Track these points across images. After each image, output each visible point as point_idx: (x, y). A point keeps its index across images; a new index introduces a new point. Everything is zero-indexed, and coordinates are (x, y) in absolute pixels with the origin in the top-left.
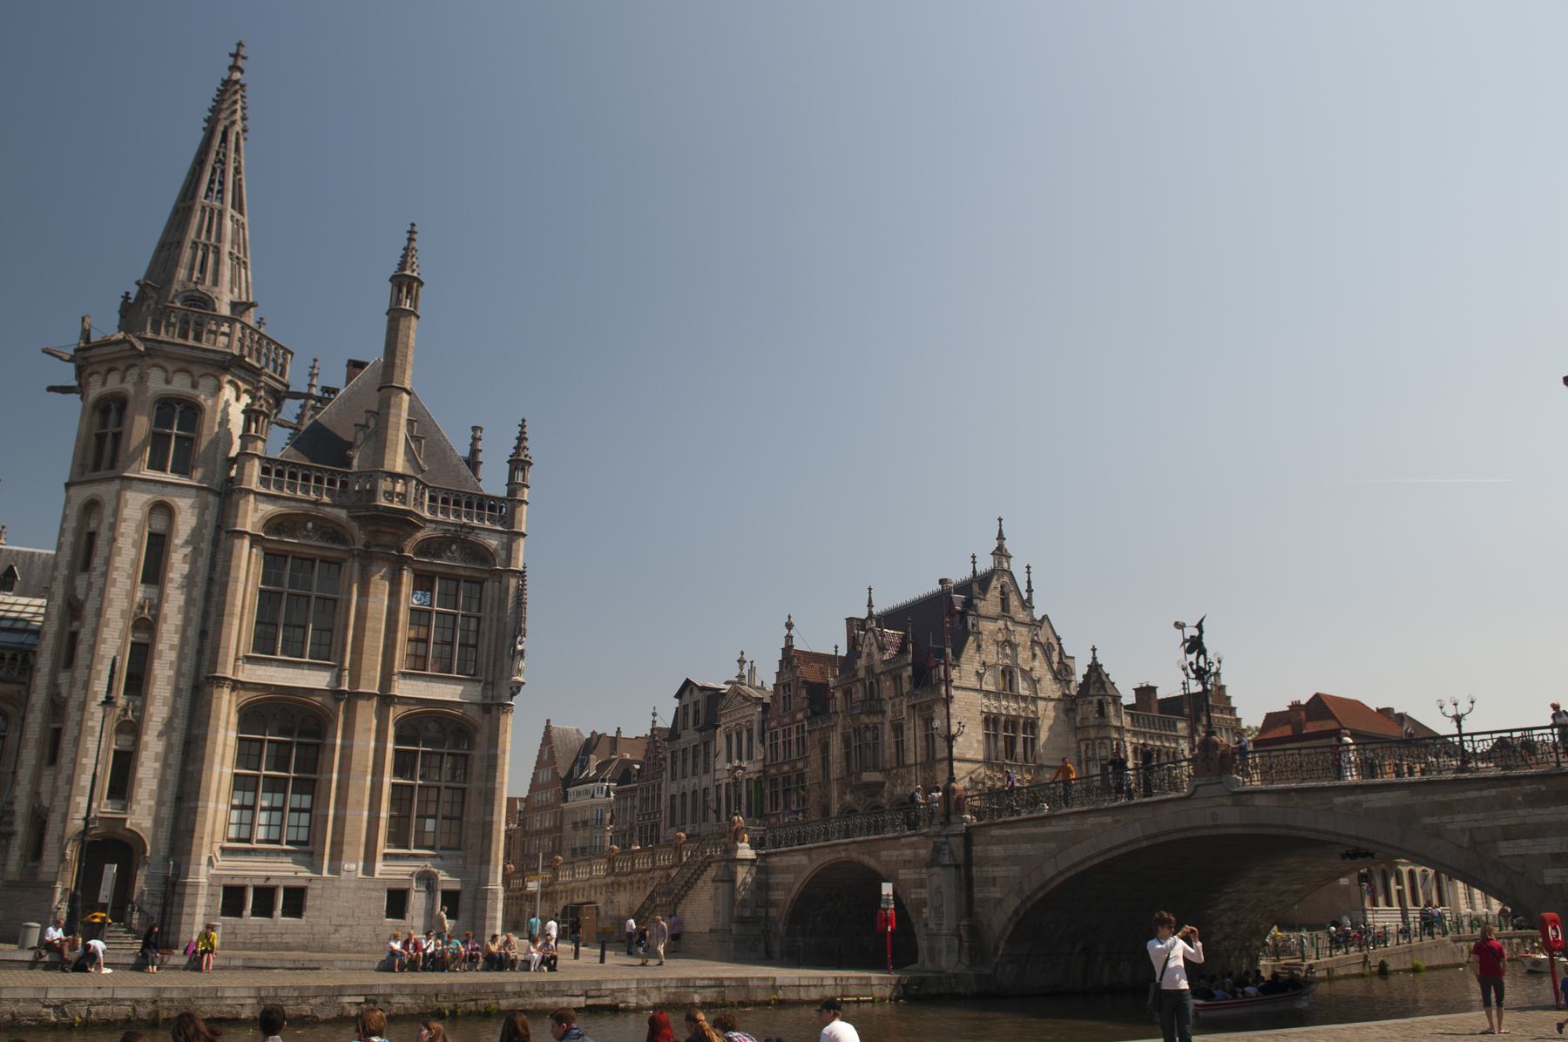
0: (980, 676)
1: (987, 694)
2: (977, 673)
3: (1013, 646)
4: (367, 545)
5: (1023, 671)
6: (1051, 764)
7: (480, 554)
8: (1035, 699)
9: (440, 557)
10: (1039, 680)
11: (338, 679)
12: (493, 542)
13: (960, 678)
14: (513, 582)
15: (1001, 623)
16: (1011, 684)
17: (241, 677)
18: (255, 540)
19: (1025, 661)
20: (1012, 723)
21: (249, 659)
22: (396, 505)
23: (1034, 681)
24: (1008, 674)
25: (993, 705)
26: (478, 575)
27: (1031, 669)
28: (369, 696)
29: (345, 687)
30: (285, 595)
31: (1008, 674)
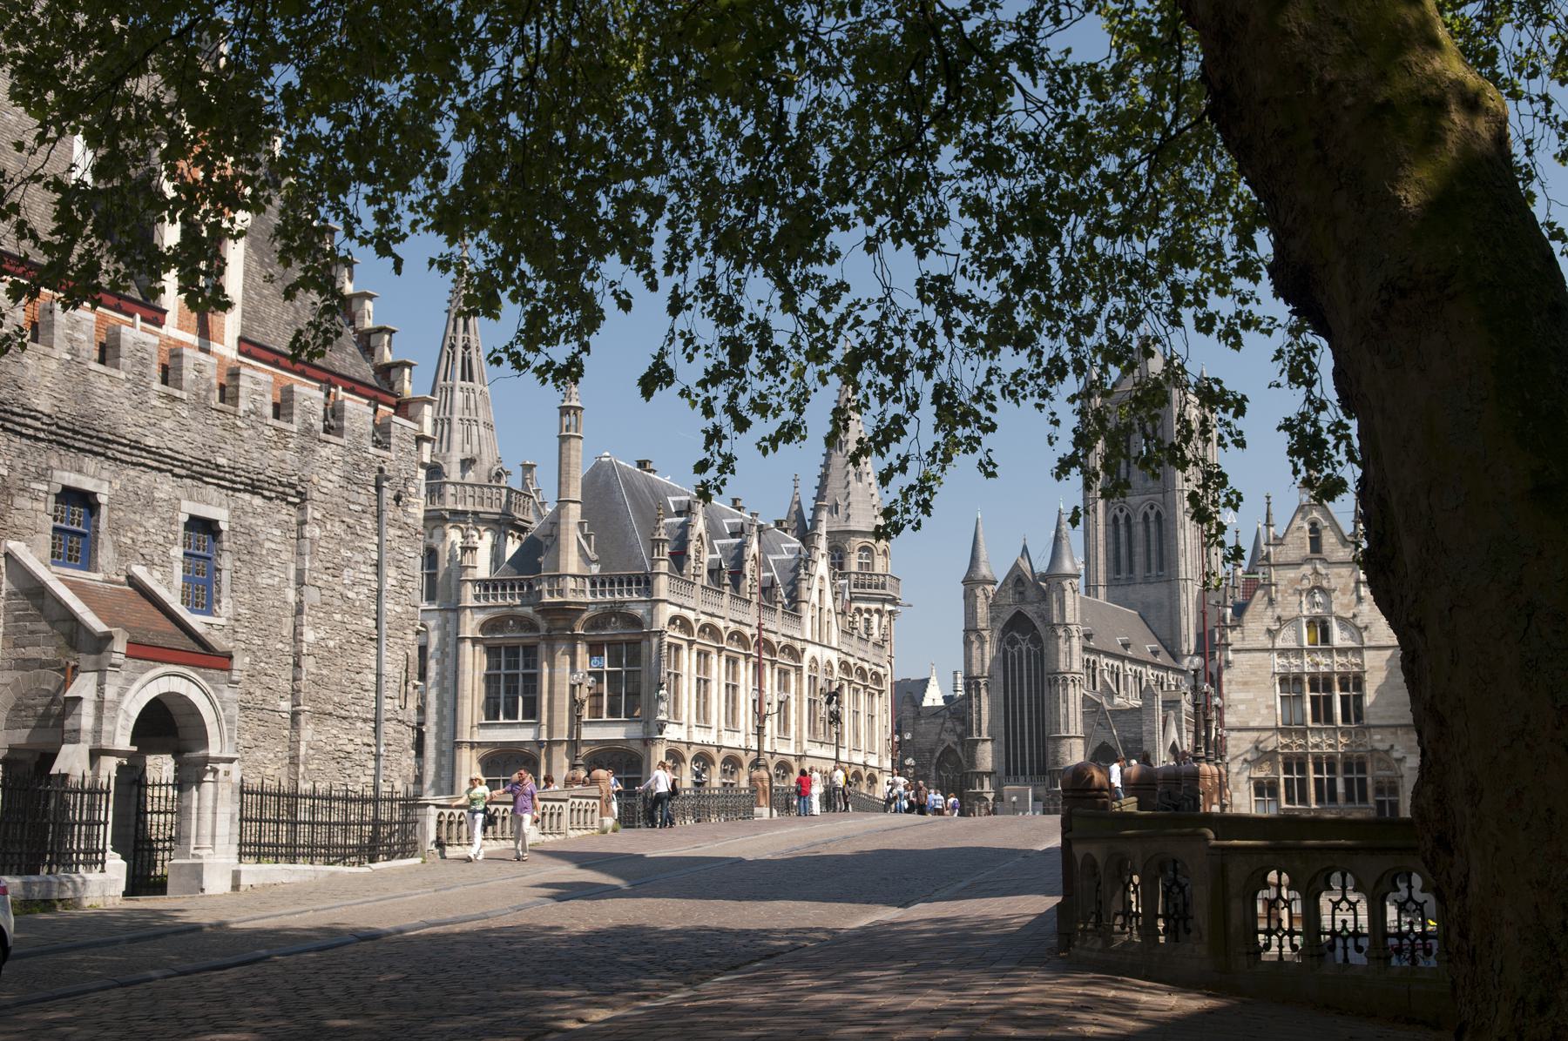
0: (1271, 633)
1: (1283, 652)
2: (1269, 631)
3: (1325, 592)
4: (549, 630)
5: (1340, 619)
6: (1384, 722)
7: (635, 622)
8: (1358, 651)
9: (604, 628)
10: (1366, 628)
11: (539, 733)
12: (640, 611)
13: (1243, 639)
14: (655, 641)
15: (1307, 569)
16: (1326, 636)
17: (476, 739)
18: (475, 641)
19: (1347, 607)
20: (1322, 683)
21: (482, 726)
22: (557, 599)
23: (1358, 629)
24: (1321, 627)
25: (1294, 665)
26: (633, 637)
27: (1355, 616)
28: (561, 742)
29: (544, 738)
30: (502, 677)
31: (1321, 627)
